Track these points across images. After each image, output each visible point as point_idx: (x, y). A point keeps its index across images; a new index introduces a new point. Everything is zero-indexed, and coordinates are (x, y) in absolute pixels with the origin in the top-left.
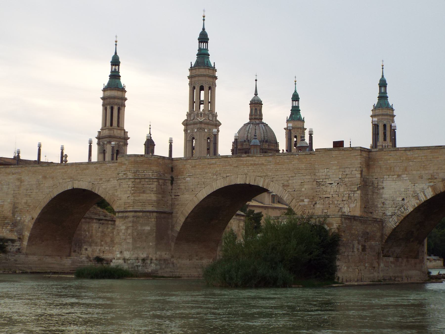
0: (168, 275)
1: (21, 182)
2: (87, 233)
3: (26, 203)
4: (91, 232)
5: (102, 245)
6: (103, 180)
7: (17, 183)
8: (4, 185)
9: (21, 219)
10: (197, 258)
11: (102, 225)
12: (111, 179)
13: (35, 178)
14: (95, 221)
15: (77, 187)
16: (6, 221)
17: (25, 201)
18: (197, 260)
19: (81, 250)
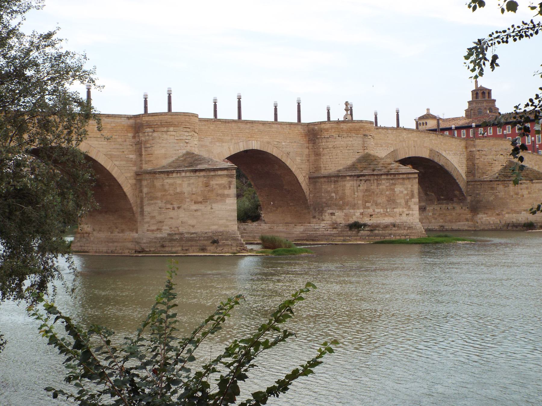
0: (77, 250)
2: (333, 195)
4: (340, 192)
5: (365, 207)
10: (118, 230)
11: (365, 181)
14: (348, 178)
18: (118, 232)
19: (322, 216)
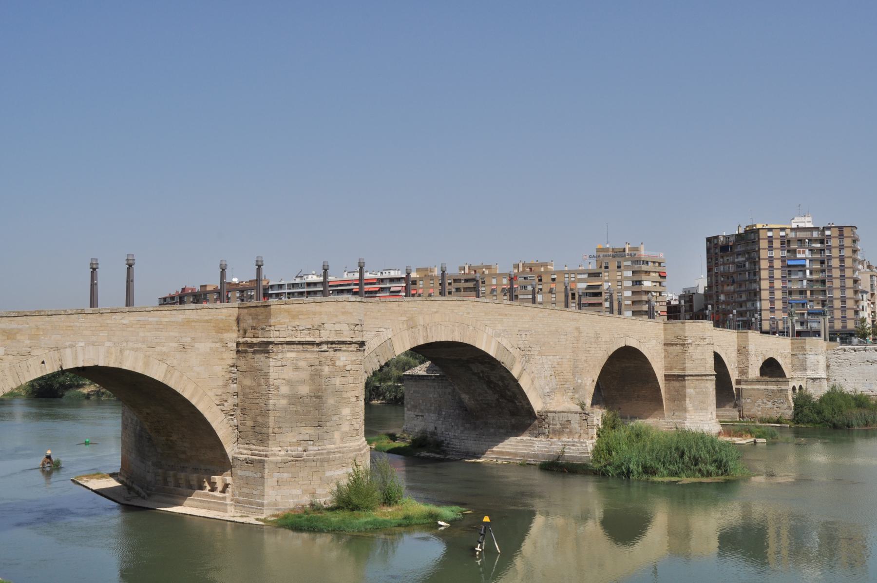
1: (580, 333)
3: (586, 361)
6: (647, 339)
7: (576, 334)
8: (562, 334)
9: (582, 383)
12: (651, 339)
13: (593, 329)
15: (628, 345)
16: (566, 386)
17: (585, 358)
